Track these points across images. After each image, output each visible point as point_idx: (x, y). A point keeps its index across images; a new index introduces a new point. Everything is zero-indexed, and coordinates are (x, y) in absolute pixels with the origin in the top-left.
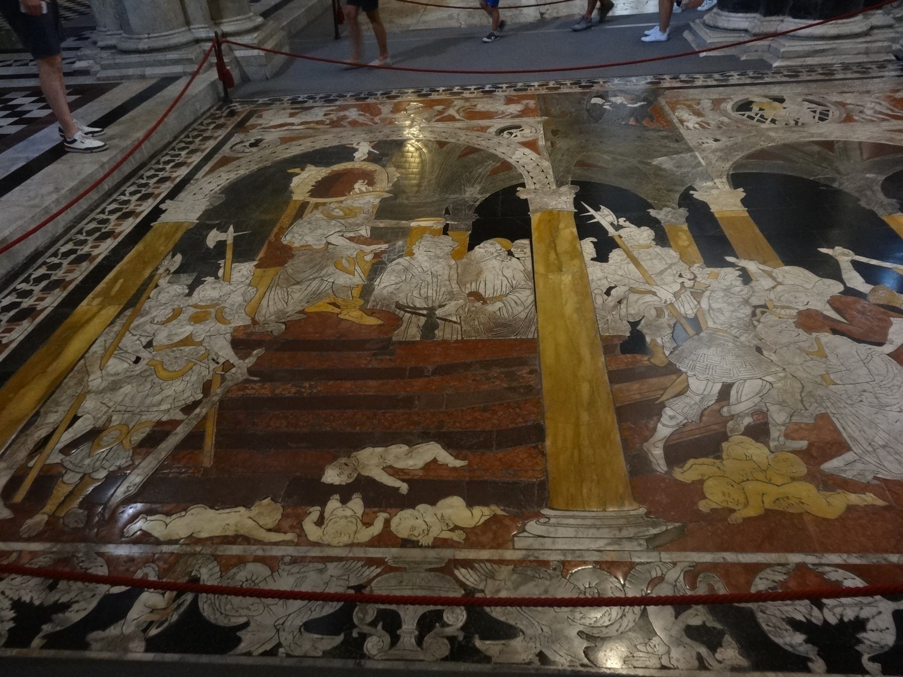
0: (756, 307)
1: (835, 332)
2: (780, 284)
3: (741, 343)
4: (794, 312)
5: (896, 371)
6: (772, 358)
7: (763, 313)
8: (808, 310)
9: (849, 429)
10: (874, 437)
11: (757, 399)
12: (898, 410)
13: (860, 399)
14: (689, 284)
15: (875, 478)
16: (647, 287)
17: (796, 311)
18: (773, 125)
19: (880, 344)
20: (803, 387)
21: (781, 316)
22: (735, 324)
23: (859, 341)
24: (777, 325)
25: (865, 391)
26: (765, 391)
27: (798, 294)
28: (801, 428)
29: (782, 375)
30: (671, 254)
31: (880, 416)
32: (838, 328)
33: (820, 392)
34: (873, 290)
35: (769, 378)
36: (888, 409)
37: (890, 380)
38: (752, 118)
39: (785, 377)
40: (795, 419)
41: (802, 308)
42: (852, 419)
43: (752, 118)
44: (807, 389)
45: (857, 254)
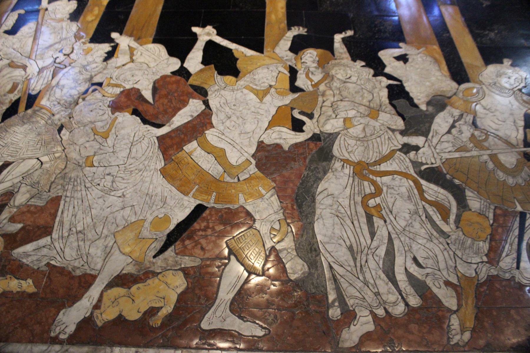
0: (93, 84)
1: (135, 112)
2: (132, 61)
3: (53, 121)
4: (118, 91)
5: (151, 154)
6: (64, 138)
7: (94, 91)
8: (133, 89)
9: (65, 215)
10: (79, 222)
11: (16, 181)
12: (120, 195)
13: (99, 182)
14: (61, 58)
15: (48, 264)
16: (26, 61)
17: (122, 89)
19: (159, 126)
20: (66, 167)
21: (106, 94)
22: (62, 102)
23: (145, 121)
24: (94, 104)
25: (109, 174)
26: (29, 173)
27: (137, 72)
28: (29, 211)
29: (57, 155)
30: (74, 27)
31: (101, 200)
32: (140, 108)
33: (73, 175)
34: (201, 71)
35: (44, 159)
36: (112, 194)
37: (137, 164)
39: (59, 157)
40: (33, 202)
41: (128, 87)
42: (76, 203)
44: (67, 170)
45: (218, 34)
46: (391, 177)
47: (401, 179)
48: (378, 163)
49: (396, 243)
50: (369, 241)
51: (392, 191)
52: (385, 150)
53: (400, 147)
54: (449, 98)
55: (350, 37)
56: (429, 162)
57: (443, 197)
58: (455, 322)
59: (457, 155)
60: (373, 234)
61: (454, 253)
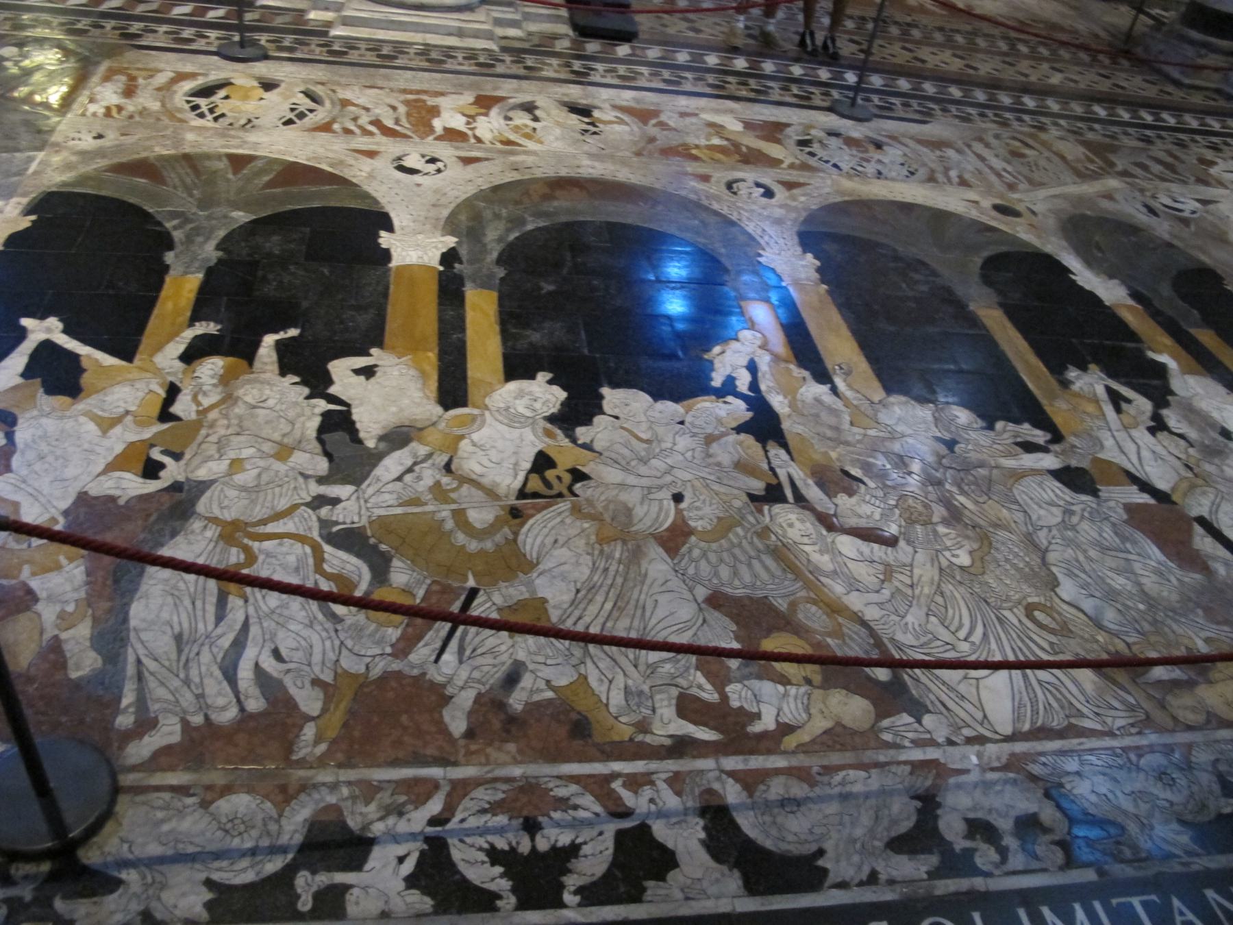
18: (211, 124)
38: (195, 108)
43: (195, 108)
46: (276, 542)
47: (292, 545)
48: (264, 522)
49: (254, 630)
50: (210, 627)
51: (273, 560)
52: (283, 504)
53: (309, 499)
54: (421, 429)
55: (293, 338)
56: (348, 521)
57: (353, 568)
58: (309, 731)
59: (399, 511)
60: (220, 618)
61: (342, 643)
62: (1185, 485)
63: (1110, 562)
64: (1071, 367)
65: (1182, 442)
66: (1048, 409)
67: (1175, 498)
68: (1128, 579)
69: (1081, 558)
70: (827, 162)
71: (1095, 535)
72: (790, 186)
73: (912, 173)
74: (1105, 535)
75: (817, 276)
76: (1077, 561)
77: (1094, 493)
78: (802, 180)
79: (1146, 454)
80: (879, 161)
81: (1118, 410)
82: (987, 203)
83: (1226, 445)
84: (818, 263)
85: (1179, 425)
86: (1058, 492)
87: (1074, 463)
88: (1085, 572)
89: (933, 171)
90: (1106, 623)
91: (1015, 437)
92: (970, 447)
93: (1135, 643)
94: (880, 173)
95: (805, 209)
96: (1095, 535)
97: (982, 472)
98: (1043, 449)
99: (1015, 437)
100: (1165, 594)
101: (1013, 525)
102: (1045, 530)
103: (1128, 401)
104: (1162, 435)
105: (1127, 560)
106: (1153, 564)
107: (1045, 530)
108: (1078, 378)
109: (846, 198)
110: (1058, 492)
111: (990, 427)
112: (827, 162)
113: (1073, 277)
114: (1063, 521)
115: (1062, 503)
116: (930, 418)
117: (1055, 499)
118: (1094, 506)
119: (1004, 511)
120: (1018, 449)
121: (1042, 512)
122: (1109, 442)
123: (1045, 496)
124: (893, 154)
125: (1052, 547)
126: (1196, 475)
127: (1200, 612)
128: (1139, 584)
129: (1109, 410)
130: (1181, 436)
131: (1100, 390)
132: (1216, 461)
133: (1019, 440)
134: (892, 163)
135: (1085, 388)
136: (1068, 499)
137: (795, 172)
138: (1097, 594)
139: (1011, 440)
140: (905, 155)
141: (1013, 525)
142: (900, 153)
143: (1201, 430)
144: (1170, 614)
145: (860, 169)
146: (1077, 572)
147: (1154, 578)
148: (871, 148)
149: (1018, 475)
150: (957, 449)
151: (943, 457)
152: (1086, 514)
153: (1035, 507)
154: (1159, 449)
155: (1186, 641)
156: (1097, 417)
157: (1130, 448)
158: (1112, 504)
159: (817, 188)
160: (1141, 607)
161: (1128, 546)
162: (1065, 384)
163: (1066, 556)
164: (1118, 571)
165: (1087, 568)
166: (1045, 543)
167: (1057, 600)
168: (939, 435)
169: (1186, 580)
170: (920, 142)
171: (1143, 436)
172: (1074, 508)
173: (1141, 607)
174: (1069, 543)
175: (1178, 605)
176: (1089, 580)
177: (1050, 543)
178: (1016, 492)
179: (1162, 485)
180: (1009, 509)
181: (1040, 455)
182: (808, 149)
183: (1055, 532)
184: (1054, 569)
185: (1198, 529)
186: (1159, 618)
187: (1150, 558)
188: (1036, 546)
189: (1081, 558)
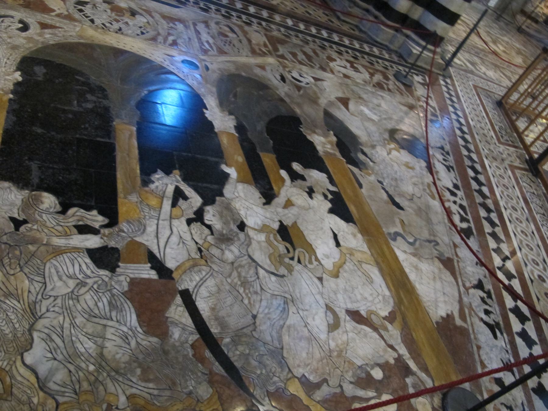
62: (188, 265)
63: (89, 328)
64: (159, 170)
65: (207, 231)
66: (120, 200)
67: (174, 275)
68: (95, 343)
69: (66, 325)
70: (87, 17)
71: (91, 303)
72: (44, 26)
73: (142, 33)
74: (100, 304)
75: (12, 87)
76: (62, 328)
77: (113, 268)
78: (58, 25)
79: (174, 239)
80: (127, 23)
81: (174, 204)
82: (179, 58)
83: (237, 234)
84: (20, 79)
85: (213, 219)
86: (84, 267)
87: (112, 244)
88: (62, 337)
89: (159, 34)
90: (51, 385)
91: (79, 220)
92: (35, 227)
93: (65, 403)
94: (120, 29)
95: (43, 43)
96: (91, 303)
97: (31, 248)
98: (94, 231)
99: (79, 220)
100: (118, 356)
101: (26, 294)
102: (52, 299)
103: (186, 198)
104: (196, 226)
105: (105, 326)
106: (125, 329)
107: (52, 299)
108: (158, 179)
109: (82, 41)
110: (84, 267)
111: (63, 212)
112: (87, 17)
113: (205, 111)
114: (72, 292)
115: (80, 277)
116: (19, 203)
117: (77, 272)
118: (107, 279)
119: (27, 282)
120: (75, 231)
121: (59, 284)
122: (151, 229)
123: (71, 270)
124: (141, 20)
125: (48, 315)
126: (202, 257)
127: (139, 371)
128: (102, 347)
129: (167, 204)
130: (209, 227)
131: (170, 189)
132: (223, 247)
133: (81, 223)
134: (134, 25)
135: (160, 188)
136: (89, 272)
137: (57, 19)
138: (60, 357)
139: (74, 223)
140: (148, 23)
141: (26, 294)
142: (145, 21)
143: (226, 223)
144: (113, 374)
145: (107, 25)
146: (54, 337)
147: (119, 341)
148: (128, 14)
149: (58, 252)
150: (22, 229)
151: (6, 234)
152: (95, 286)
153: (56, 278)
154: (187, 237)
155: (111, 398)
156: (154, 209)
157: (165, 233)
158: (122, 278)
159: (65, 31)
160: (92, 368)
161: (114, 314)
162: (146, 182)
163: (55, 323)
164: (90, 336)
165: (66, 332)
166: (44, 310)
167: (19, 363)
168: (16, 216)
169: (144, 343)
170: (164, 17)
171: (180, 225)
172: (88, 281)
173: (92, 368)
174: (67, 311)
175: (123, 365)
176: (60, 344)
177: (48, 311)
178: (48, 265)
179: (170, 264)
180: (31, 280)
181: (89, 236)
182: (80, 7)
183: (59, 301)
184: (35, 335)
185: (178, 299)
186: (101, 378)
187: (126, 325)
188: (33, 313)
189: (66, 325)
